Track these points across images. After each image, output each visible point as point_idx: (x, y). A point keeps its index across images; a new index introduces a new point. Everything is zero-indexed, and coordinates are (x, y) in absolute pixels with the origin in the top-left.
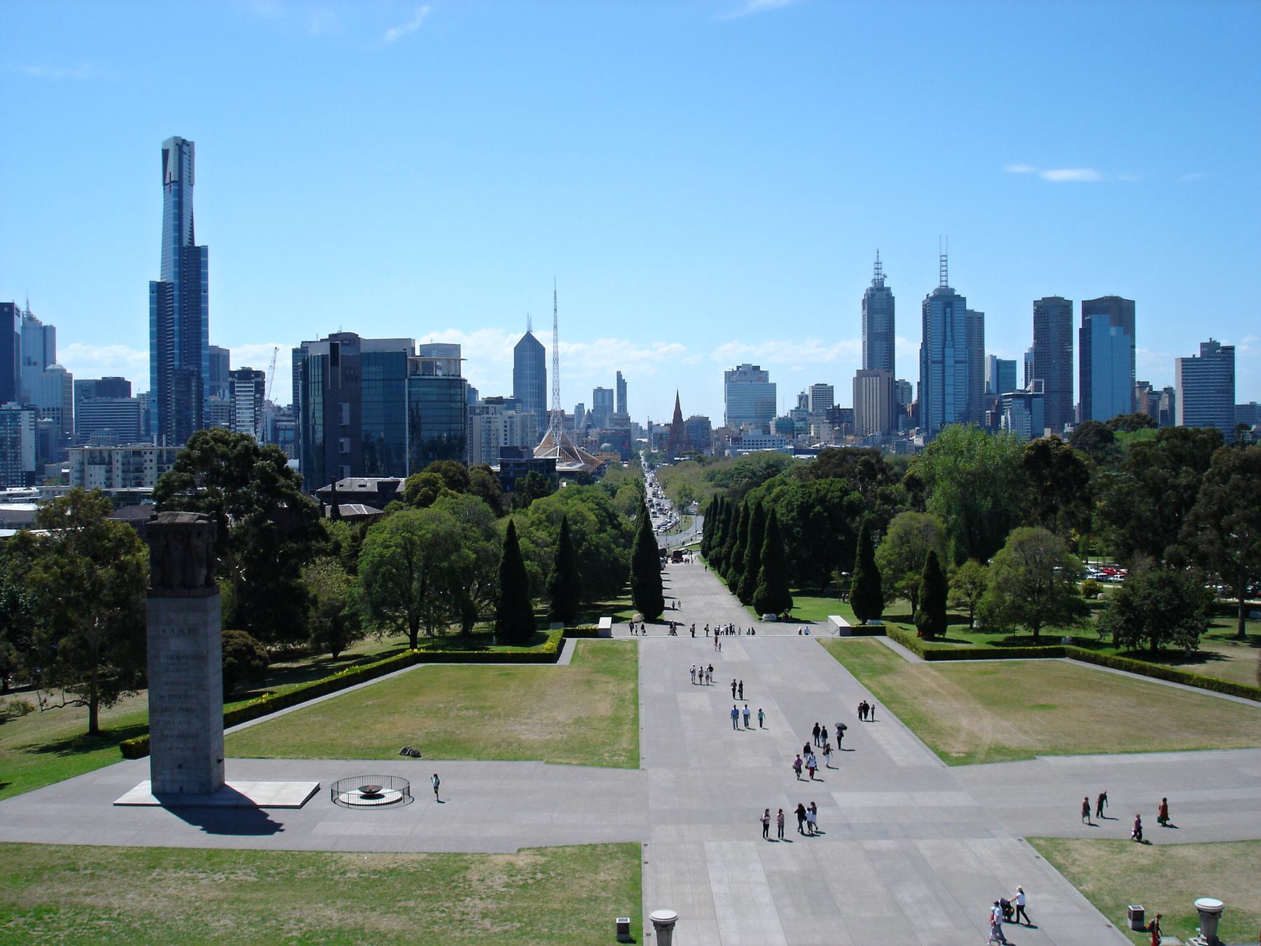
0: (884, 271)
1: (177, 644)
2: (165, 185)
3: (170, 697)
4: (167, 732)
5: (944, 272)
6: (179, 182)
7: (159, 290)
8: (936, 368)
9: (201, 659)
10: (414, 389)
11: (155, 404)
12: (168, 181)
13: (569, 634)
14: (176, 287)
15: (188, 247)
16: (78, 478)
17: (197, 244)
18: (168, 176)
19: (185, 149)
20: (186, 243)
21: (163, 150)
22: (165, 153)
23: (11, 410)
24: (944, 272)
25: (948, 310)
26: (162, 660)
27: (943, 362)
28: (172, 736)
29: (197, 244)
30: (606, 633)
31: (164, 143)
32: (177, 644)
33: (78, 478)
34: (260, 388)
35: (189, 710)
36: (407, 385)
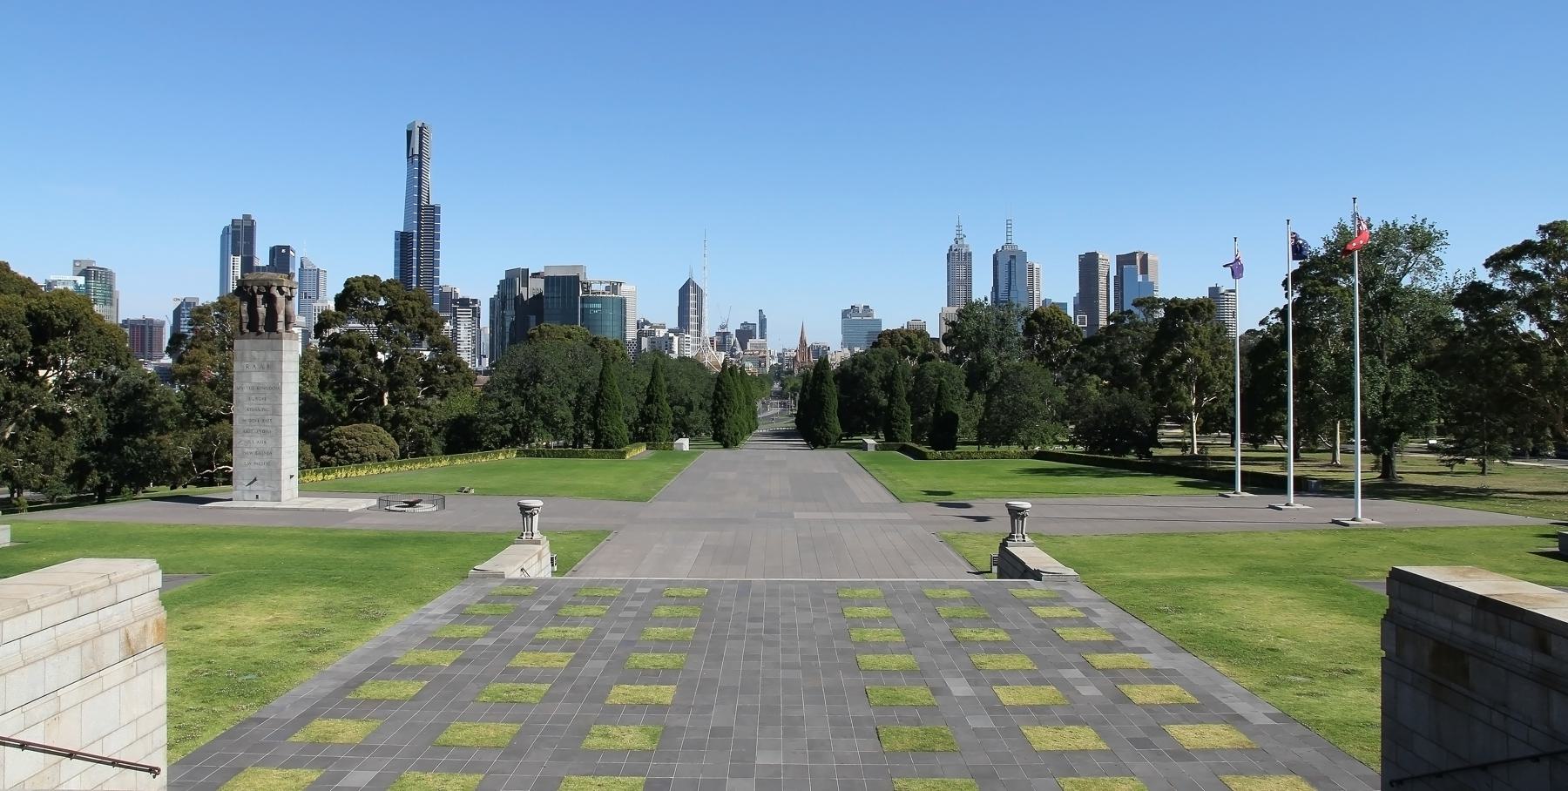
1: (258, 378)
2: (408, 158)
3: (251, 420)
4: (247, 450)
6: (420, 156)
9: (276, 389)
10: (586, 306)
12: (410, 155)
14: (415, 236)
20: (424, 203)
22: (409, 134)
26: (246, 390)
28: (251, 453)
32: (258, 378)
34: (476, 313)
35: (264, 431)
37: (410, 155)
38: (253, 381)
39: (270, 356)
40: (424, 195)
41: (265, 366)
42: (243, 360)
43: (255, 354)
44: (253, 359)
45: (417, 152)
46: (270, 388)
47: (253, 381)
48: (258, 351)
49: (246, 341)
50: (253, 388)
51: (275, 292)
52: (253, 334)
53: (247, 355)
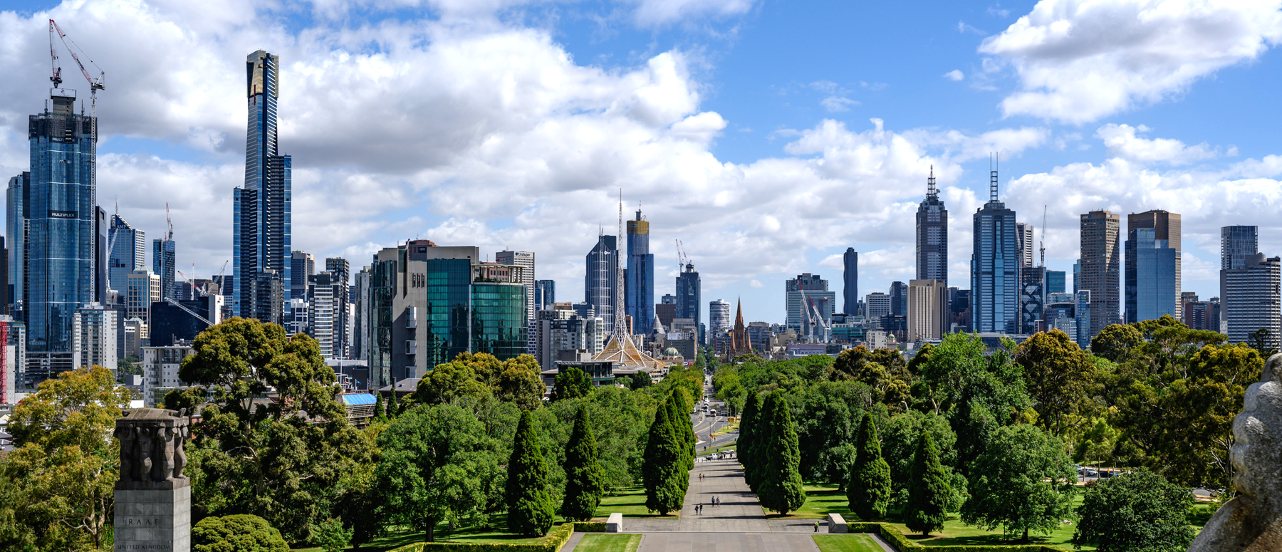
0: (937, 187)
1: (143, 535)
2: (249, 97)
5: (994, 188)
6: (265, 94)
7: (244, 200)
8: (986, 279)
11: (239, 306)
13: (578, 529)
14: (260, 195)
15: (272, 157)
16: (151, 376)
17: (280, 154)
18: (252, 88)
19: (270, 63)
20: (270, 153)
21: (248, 63)
22: (250, 67)
23: (94, 310)
24: (994, 188)
25: (998, 223)
27: (993, 273)
29: (280, 154)
30: (613, 528)
31: (249, 57)
32: (143, 535)
33: (151, 376)
36: (470, 290)
37: (252, 93)
38: (138, 538)
39: (158, 509)
40: (270, 145)
41: (152, 520)
42: (125, 514)
43: (140, 507)
44: (137, 513)
45: (260, 90)
46: (160, 547)
47: (138, 538)
48: (144, 504)
49: (128, 491)
50: (137, 547)
51: (162, 432)
52: (136, 484)
53: (130, 507)
